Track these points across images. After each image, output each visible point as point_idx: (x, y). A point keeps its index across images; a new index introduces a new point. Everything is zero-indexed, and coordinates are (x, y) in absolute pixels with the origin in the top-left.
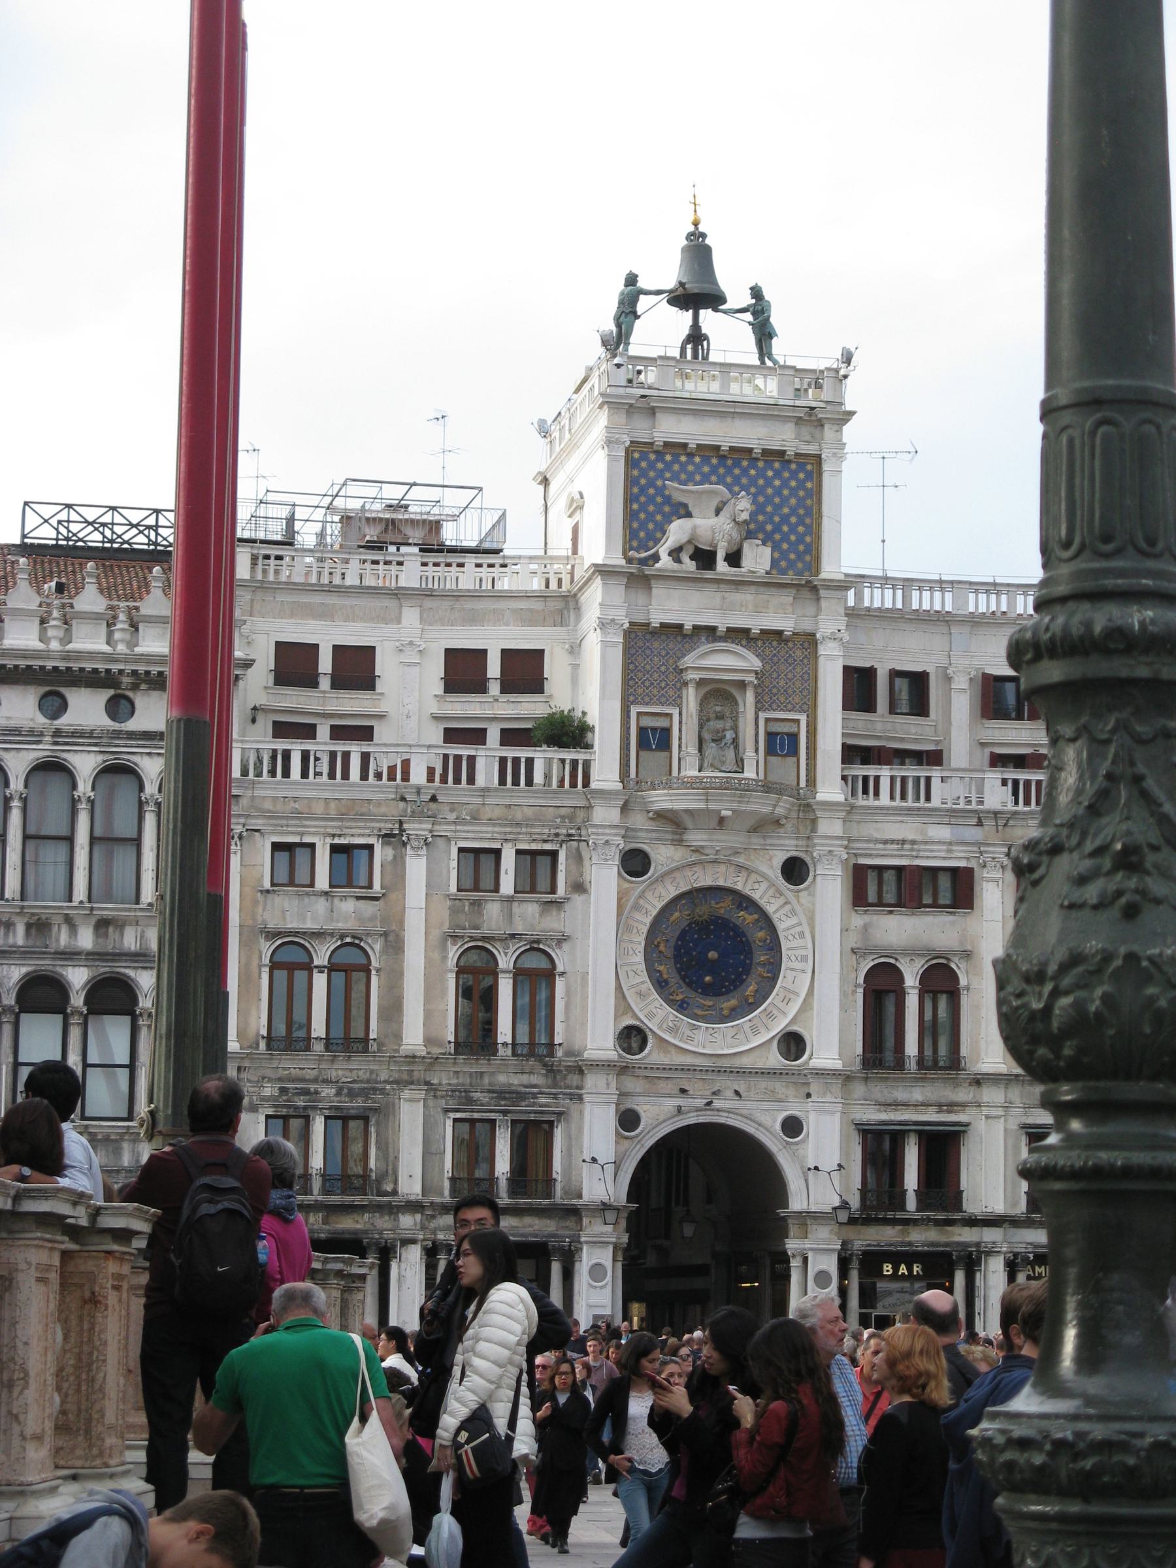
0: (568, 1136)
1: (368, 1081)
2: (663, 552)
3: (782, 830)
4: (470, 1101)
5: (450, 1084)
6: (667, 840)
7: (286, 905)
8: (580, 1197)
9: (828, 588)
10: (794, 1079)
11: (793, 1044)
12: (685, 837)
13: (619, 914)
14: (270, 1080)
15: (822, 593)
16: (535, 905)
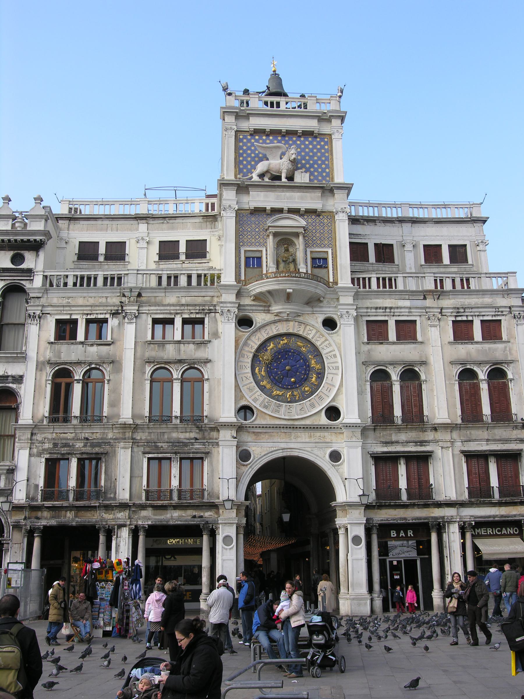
1: (102, 439)
3: (321, 304)
4: (157, 449)
8: (219, 498)
11: (333, 412)
12: (270, 308)
15: (335, 191)
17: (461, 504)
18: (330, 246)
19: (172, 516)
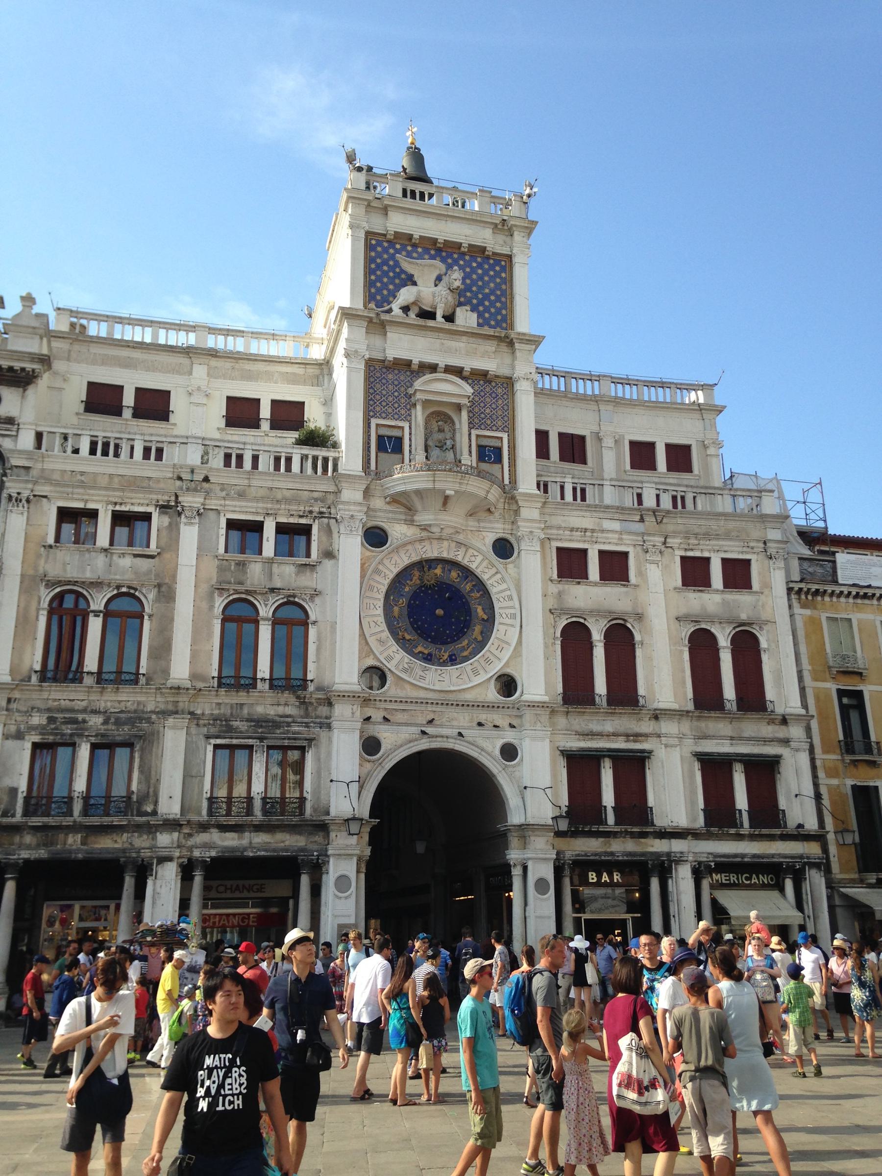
0: (318, 759)
1: (135, 711)
2: (396, 306)
3: (491, 518)
4: (229, 730)
5: (212, 714)
6: (401, 520)
7: (68, 559)
8: (328, 813)
9: (522, 341)
10: (509, 712)
11: (508, 685)
12: (416, 518)
13: (363, 576)
14: (39, 710)
15: (517, 345)
16: (292, 567)
17: (695, 834)
18: (506, 429)
19: (251, 843)
